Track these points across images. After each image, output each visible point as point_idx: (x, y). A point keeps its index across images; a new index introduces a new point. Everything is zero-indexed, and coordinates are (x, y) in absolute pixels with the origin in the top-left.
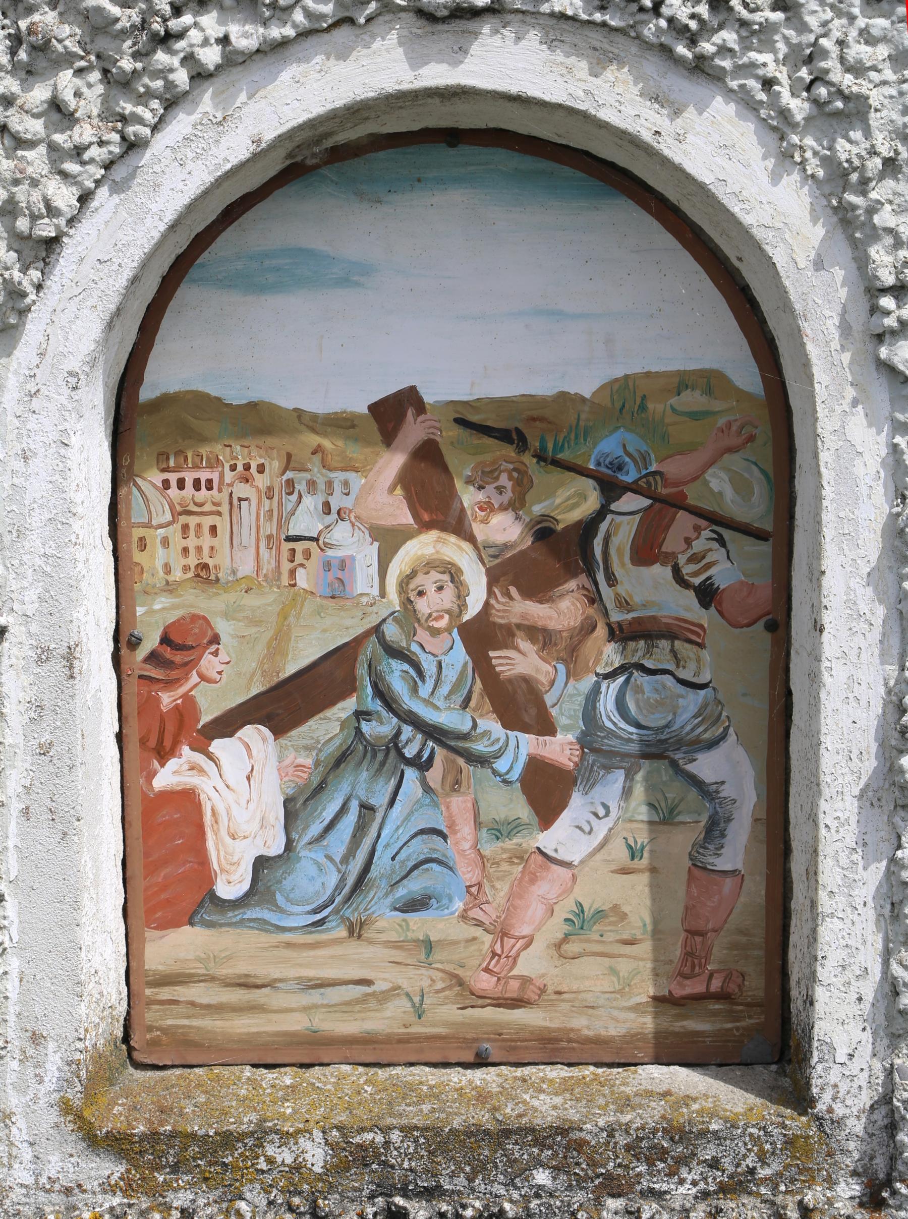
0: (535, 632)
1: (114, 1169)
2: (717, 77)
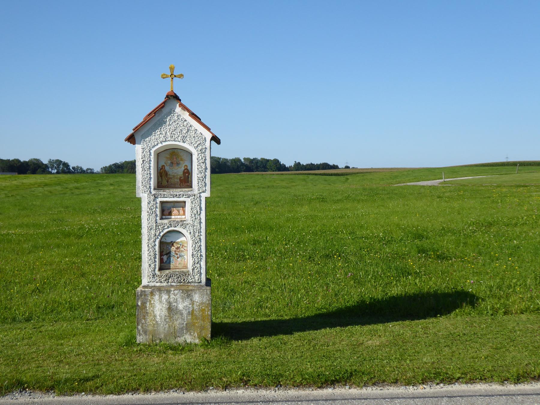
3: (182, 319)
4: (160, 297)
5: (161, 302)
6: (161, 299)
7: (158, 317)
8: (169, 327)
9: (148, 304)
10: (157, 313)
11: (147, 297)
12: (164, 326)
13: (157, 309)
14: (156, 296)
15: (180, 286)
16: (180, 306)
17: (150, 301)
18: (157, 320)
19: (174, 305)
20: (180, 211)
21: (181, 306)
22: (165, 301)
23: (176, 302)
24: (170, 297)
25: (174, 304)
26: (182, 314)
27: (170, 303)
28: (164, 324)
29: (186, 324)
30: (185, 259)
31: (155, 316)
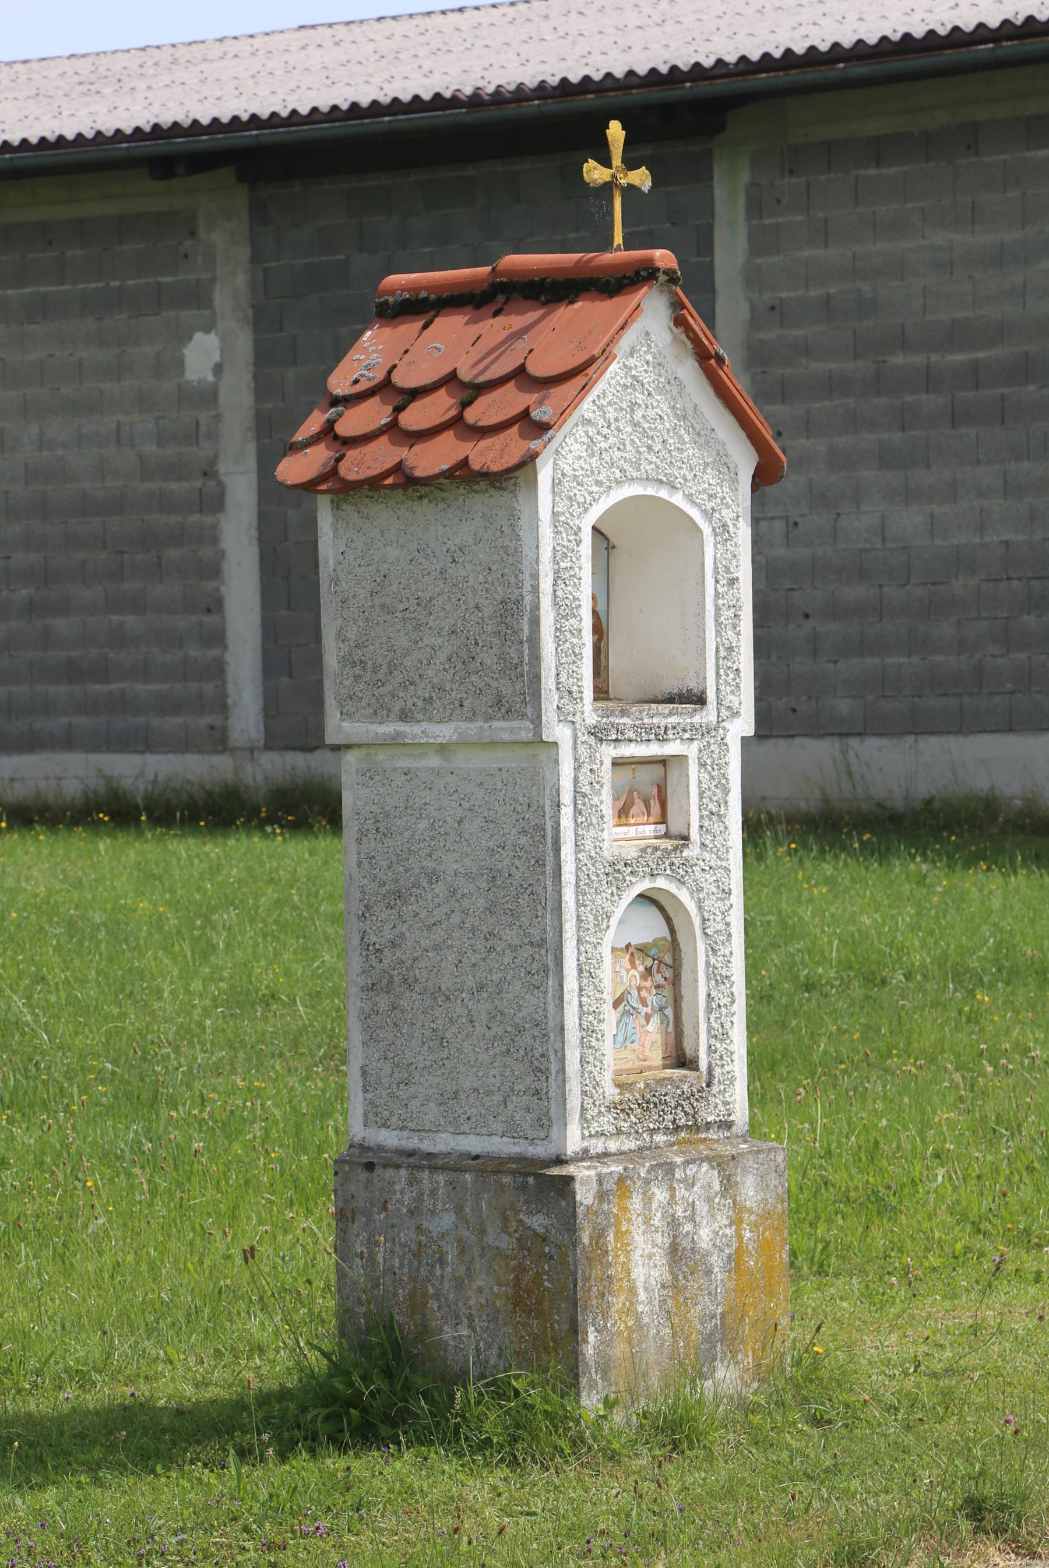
0: (646, 988)
1: (618, 1091)
2: (684, 883)
3: (710, 1293)
4: (648, 1199)
5: (647, 1221)
6: (650, 1210)
7: (642, 1296)
8: (674, 1335)
9: (611, 1238)
10: (639, 1273)
11: (609, 1203)
12: (658, 1332)
13: (636, 1256)
14: (634, 1194)
15: (679, 1143)
16: (704, 1237)
17: (618, 1224)
18: (640, 1309)
19: (688, 1233)
20: (652, 802)
21: (705, 1236)
22: (659, 1215)
23: (692, 1219)
24: (673, 1196)
25: (686, 1229)
26: (709, 1272)
27: (673, 1223)
28: (660, 1323)
29: (723, 1315)
30: (668, 1024)
31: (633, 1291)
